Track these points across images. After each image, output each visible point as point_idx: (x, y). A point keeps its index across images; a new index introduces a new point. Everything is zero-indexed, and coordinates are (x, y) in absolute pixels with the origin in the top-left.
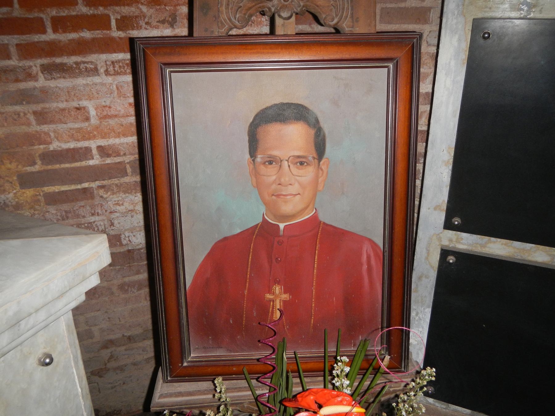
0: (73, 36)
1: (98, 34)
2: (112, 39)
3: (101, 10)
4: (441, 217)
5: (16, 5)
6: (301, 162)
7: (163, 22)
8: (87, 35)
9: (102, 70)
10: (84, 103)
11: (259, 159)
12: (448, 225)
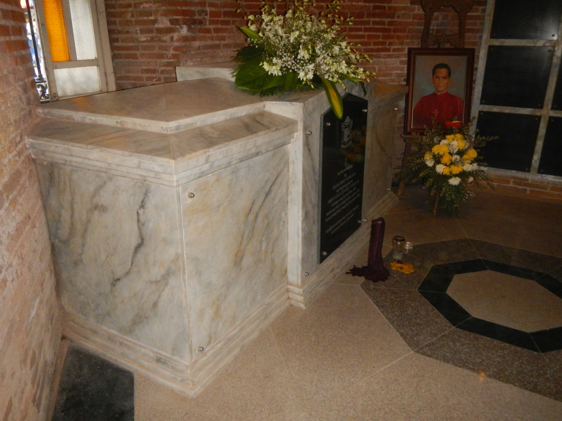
0: (377, 47)
1: (383, 47)
2: (386, 48)
3: (385, 40)
4: (479, 102)
5: (366, 38)
6: (445, 78)
7: (399, 44)
8: (380, 47)
9: (382, 57)
10: (375, 66)
11: (435, 76)
12: (481, 103)
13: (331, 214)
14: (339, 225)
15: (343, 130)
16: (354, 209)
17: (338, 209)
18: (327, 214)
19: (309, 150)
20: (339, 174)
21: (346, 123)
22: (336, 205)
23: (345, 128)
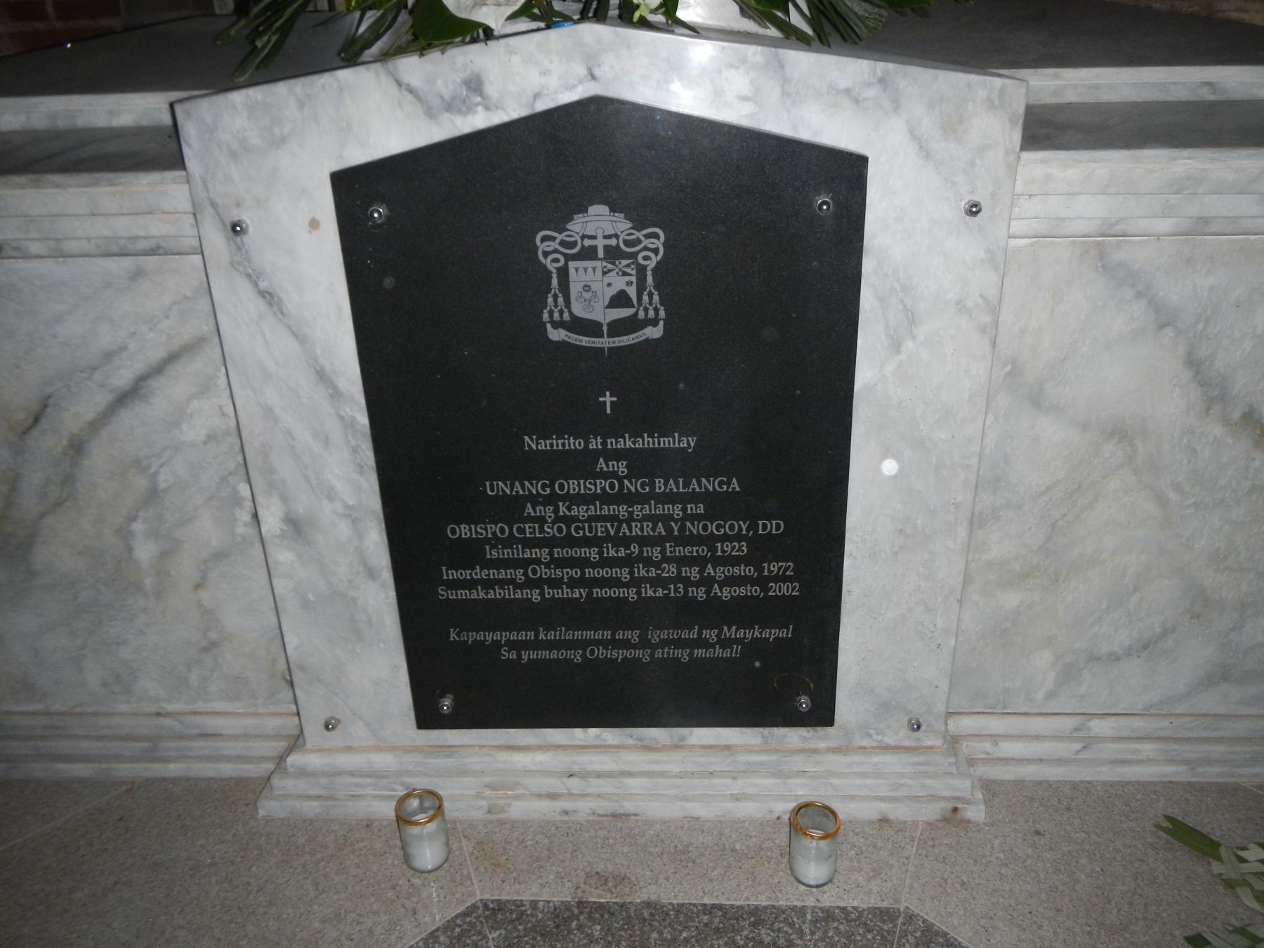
13: (488, 584)
14: (582, 644)
15: (551, 267)
16: (731, 632)
17: (555, 583)
18: (453, 575)
19: (268, 296)
20: (530, 442)
21: (594, 237)
22: (538, 561)
23: (568, 258)
